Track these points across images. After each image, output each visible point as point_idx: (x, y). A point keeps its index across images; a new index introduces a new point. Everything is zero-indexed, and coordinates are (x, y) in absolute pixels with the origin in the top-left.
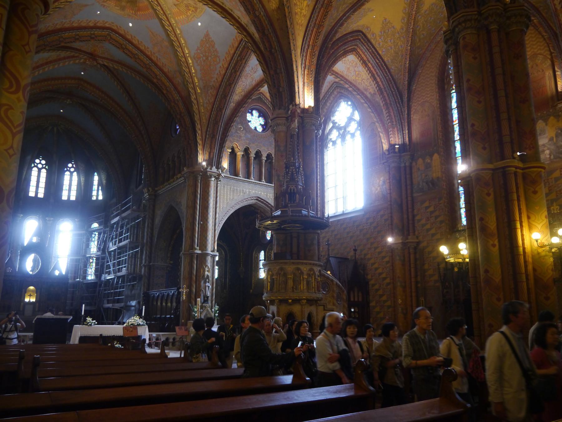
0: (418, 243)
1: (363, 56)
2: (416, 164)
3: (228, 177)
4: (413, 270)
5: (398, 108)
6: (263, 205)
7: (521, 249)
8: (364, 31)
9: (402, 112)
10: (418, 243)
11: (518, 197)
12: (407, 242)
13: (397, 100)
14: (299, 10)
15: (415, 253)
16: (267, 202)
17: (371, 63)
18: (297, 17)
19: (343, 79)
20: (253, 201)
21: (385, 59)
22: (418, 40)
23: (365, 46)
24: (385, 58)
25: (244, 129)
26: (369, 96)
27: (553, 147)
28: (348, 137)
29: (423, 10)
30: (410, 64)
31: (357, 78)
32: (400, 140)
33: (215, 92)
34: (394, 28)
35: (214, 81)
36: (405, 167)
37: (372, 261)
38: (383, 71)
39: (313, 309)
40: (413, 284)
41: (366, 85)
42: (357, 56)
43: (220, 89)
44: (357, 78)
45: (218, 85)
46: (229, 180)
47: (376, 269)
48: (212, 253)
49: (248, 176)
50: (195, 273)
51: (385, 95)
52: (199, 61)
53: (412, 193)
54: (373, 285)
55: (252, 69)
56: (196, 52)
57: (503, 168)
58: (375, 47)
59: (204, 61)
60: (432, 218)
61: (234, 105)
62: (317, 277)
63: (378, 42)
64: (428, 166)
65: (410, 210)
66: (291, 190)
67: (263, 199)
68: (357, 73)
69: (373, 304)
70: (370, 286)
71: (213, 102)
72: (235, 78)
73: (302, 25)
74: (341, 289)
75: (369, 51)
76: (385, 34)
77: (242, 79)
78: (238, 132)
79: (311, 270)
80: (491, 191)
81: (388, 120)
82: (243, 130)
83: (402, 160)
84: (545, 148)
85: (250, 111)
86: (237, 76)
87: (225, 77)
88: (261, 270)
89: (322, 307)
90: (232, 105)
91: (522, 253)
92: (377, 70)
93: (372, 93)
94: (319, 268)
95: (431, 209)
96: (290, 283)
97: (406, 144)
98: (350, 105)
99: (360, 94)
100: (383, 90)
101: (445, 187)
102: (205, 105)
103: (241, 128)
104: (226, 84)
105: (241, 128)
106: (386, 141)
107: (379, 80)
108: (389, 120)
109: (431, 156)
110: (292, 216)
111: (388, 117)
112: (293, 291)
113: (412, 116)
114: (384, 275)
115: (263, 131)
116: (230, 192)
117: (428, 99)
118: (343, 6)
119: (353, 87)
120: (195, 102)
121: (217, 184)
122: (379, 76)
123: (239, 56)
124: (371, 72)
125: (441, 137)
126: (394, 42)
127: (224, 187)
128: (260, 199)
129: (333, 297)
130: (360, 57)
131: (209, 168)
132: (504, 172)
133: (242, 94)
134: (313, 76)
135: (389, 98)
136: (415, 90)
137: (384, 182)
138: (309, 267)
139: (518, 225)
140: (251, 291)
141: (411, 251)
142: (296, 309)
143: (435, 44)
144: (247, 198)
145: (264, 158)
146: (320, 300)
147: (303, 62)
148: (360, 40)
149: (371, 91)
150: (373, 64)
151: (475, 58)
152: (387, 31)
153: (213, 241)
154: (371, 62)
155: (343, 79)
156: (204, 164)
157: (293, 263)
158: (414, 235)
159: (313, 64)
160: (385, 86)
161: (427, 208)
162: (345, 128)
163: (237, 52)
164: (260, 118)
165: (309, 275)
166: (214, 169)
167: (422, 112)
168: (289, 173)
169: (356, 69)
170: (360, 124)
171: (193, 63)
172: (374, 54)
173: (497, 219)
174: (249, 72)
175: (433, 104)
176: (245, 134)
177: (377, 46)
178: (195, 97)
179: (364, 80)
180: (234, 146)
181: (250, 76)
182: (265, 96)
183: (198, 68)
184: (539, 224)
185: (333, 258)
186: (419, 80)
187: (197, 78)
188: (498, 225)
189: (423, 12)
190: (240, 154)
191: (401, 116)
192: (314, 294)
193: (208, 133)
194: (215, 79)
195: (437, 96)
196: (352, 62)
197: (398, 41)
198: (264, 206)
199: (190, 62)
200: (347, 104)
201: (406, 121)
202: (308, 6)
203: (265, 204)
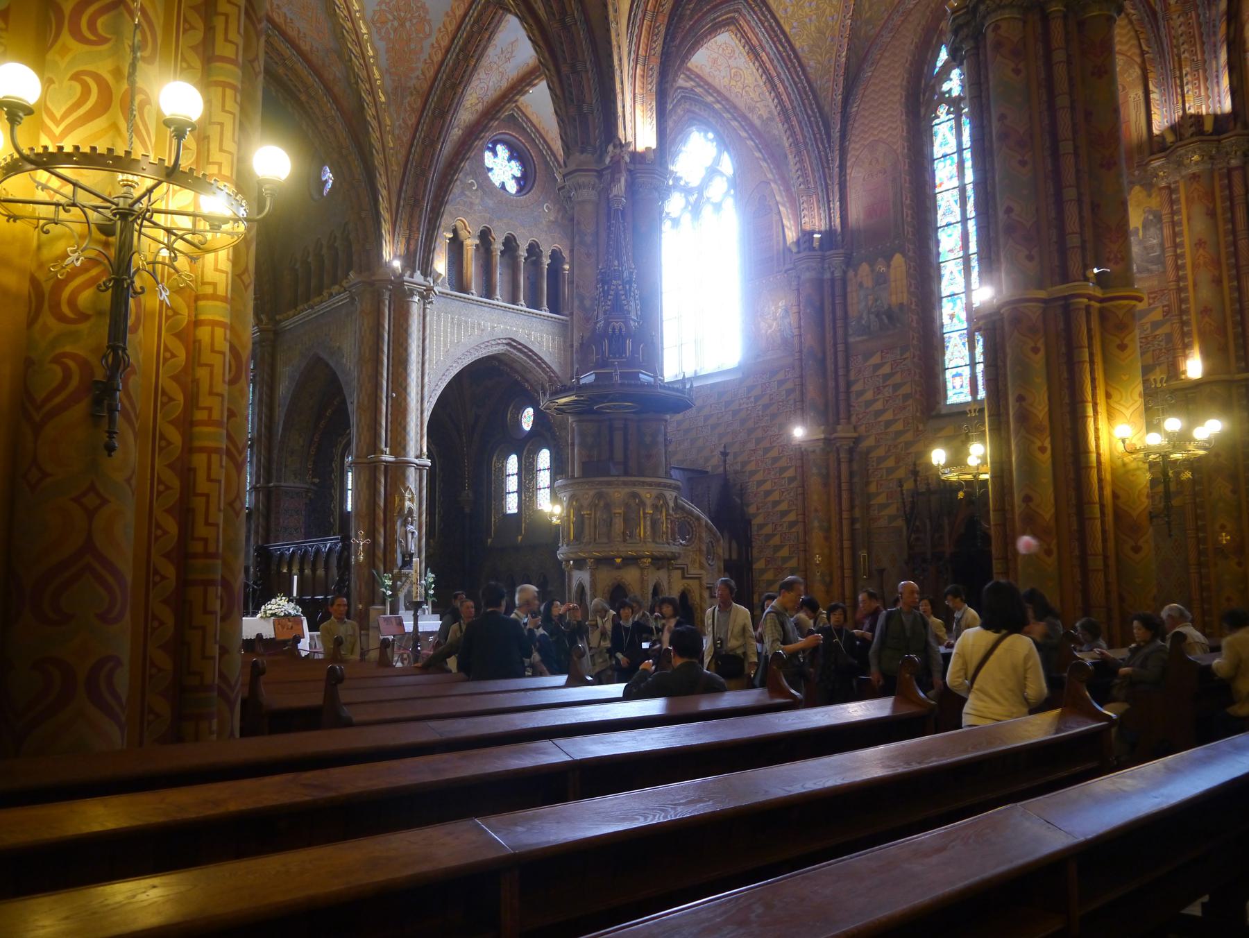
0: (857, 441)
1: (750, 35)
2: (856, 275)
3: (447, 294)
4: (845, 495)
5: (819, 152)
6: (521, 356)
7: (1093, 457)
9: (828, 161)
10: (857, 441)
11: (1091, 355)
12: (835, 438)
13: (818, 136)
15: (850, 461)
16: (531, 351)
17: (769, 51)
19: (702, 83)
21: (797, 45)
22: (867, 6)
23: (755, 13)
24: (797, 43)
25: (480, 186)
26: (757, 122)
28: (707, 210)
30: (848, 59)
31: (733, 83)
32: (823, 223)
33: (419, 103)
35: (418, 76)
36: (833, 280)
37: (759, 477)
38: (792, 69)
39: (662, 575)
40: (845, 523)
41: (752, 99)
42: (739, 35)
43: (431, 97)
44: (733, 83)
45: (425, 86)
47: (768, 493)
48: (417, 461)
49: (488, 292)
50: (382, 504)
51: (795, 123)
52: (383, 31)
53: (846, 335)
54: (761, 527)
56: (378, 8)
57: (1065, 298)
58: (778, 16)
59: (395, 30)
60: (887, 389)
61: (460, 132)
62: (671, 511)
64: (881, 280)
65: (841, 372)
66: (614, 329)
67: (520, 344)
68: (733, 71)
69: (759, 565)
70: (755, 528)
71: (414, 126)
72: (465, 72)
74: (715, 535)
77: (479, 74)
79: (660, 496)
80: (1041, 344)
81: (798, 178)
82: (476, 190)
83: (826, 266)
85: (490, 146)
86: (470, 68)
87: (443, 68)
88: (511, 495)
89: (680, 571)
90: (456, 133)
91: (1095, 464)
92: (778, 67)
93: (765, 118)
94: (674, 494)
95: (886, 369)
96: (619, 525)
97: (836, 230)
98: (712, 141)
99: (739, 119)
100: (790, 112)
101: (914, 324)
102: (397, 132)
103: (472, 184)
104: (444, 85)
105: (472, 184)
106: (792, 222)
107: (781, 89)
108: (801, 179)
109: (888, 259)
110: (621, 385)
111: (799, 173)
112: (625, 541)
113: (848, 171)
114: (783, 506)
115: (519, 191)
116: (452, 328)
117: (885, 136)
119: (723, 102)
120: (374, 123)
121: (424, 309)
122: (782, 81)
123: (477, 21)
124: (765, 71)
125: (909, 219)
126: (818, 8)
127: (439, 316)
128: (515, 344)
129: (700, 550)
130: (743, 37)
131: (408, 273)
132: (1066, 306)
133: (477, 107)
134: (654, 82)
135: (802, 130)
136: (856, 115)
137: (786, 311)
138: (655, 492)
139: (1090, 411)
140: (489, 541)
141: (843, 455)
142: (630, 576)
143: (902, 16)
144: (488, 342)
145: (523, 253)
146: (674, 557)
147: (633, 49)
149: (761, 112)
151: (1017, 71)
153: (419, 435)
154: (768, 49)
155: (702, 83)
156: (397, 264)
157: (625, 483)
158: (849, 421)
159: (654, 55)
160: (795, 104)
162: (700, 190)
163: (471, 11)
164: (513, 162)
165: (655, 507)
166: (418, 278)
167: (870, 164)
168: (609, 295)
169: (732, 63)
170: (736, 183)
171: (369, 33)
172: (774, 31)
173: (1050, 399)
174: (496, 59)
175: (895, 147)
176: (482, 199)
177: (780, 14)
178: (374, 113)
179: (747, 88)
180: (459, 224)
181: (497, 69)
182: (523, 113)
183: (382, 45)
184: (1128, 408)
185: (677, 471)
186: (866, 93)
187: (379, 69)
188: (1050, 410)
190: (471, 243)
191: (826, 170)
192: (666, 545)
193: (403, 195)
194: (419, 73)
195: (903, 131)
196: (724, 46)
198: (525, 358)
199: (364, 31)
200: (705, 136)
201: (836, 180)
203: (525, 354)
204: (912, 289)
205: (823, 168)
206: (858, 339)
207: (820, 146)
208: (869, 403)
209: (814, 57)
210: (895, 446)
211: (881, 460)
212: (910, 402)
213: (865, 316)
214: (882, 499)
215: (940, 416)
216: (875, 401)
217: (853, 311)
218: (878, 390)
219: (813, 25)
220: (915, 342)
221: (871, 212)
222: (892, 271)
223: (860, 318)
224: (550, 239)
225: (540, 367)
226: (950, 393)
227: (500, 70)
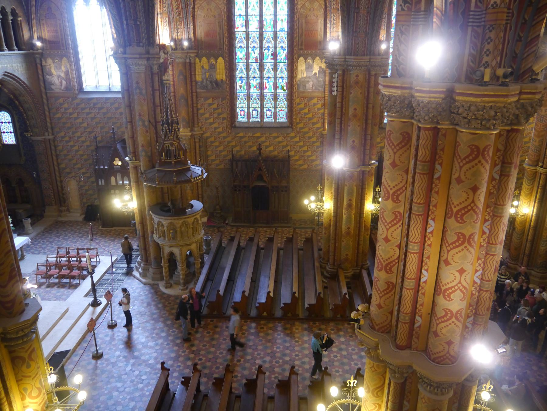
2: (200, 62)
16: (14, 75)
27: (315, 81)
36: (190, 63)
64: (213, 67)
67: (9, 73)
84: (310, 80)
95: (215, 106)
96: (191, 231)
101: (228, 89)
109: (216, 59)
125: (226, 43)
161: (210, 104)
167: (208, 10)
175: (220, 7)
204: (227, 74)
206: (202, 91)
208: (207, 119)
210: (219, 138)
211: (212, 142)
212: (225, 121)
213: (205, 81)
214: (213, 157)
215: (235, 127)
216: (209, 118)
217: (199, 78)
218: (211, 114)
220: (228, 97)
221: (208, 34)
222: (218, 65)
223: (202, 82)
226: (239, 117)
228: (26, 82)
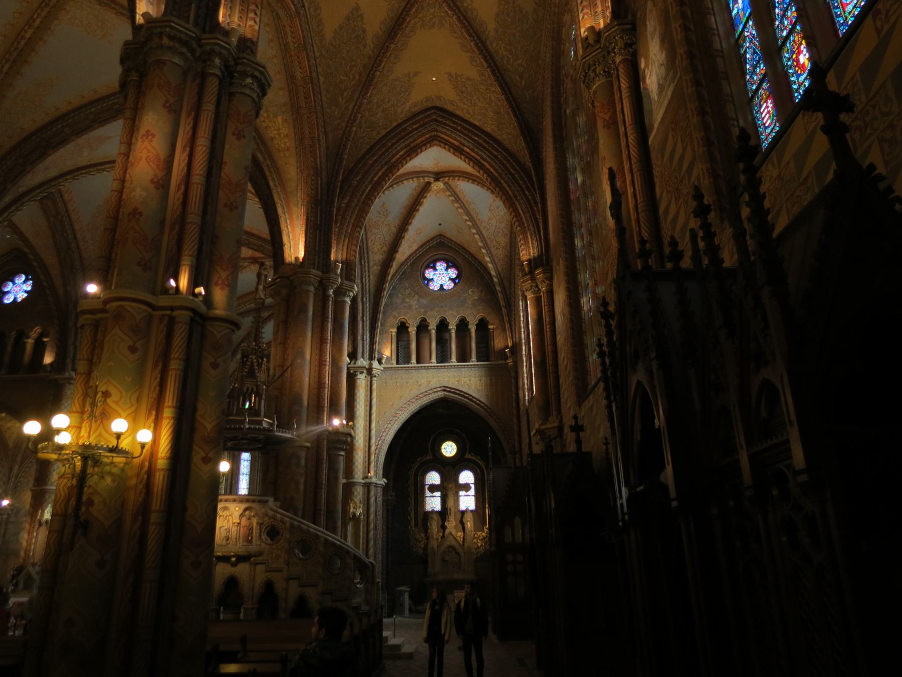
1: (452, 141)
6: (457, 396)
8: (438, 104)
13: (523, 186)
14: (275, 132)
18: (275, 143)
20: (439, 393)
21: (489, 130)
22: (518, 78)
29: (489, 31)
34: (470, 80)
42: (442, 145)
46: (393, 371)
49: (443, 357)
51: (505, 185)
55: (380, 214)
61: (379, 267)
63: (464, 110)
73: (288, 149)
75: (456, 129)
76: (465, 95)
78: (407, 300)
107: (488, 166)
111: (515, 219)
118: (346, 94)
122: (484, 159)
126: (485, 99)
128: (449, 389)
130: (446, 144)
133: (383, 250)
144: (426, 392)
148: (436, 120)
150: (471, 147)
152: (464, 89)
153: (367, 464)
154: (467, 144)
176: (418, 301)
177: (467, 117)
182: (446, 238)
189: (492, 34)
191: (535, 208)
197: (489, 95)
202: (285, 121)
205: (531, 207)
207: (527, 193)
209: (504, 132)
219: (490, 112)
224: (475, 312)
225: (473, 401)
227: (385, 223)
228: (482, 399)
